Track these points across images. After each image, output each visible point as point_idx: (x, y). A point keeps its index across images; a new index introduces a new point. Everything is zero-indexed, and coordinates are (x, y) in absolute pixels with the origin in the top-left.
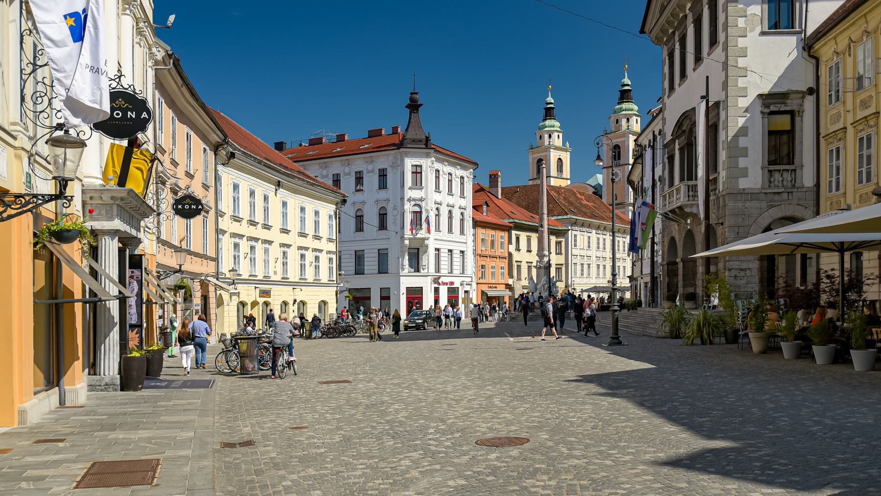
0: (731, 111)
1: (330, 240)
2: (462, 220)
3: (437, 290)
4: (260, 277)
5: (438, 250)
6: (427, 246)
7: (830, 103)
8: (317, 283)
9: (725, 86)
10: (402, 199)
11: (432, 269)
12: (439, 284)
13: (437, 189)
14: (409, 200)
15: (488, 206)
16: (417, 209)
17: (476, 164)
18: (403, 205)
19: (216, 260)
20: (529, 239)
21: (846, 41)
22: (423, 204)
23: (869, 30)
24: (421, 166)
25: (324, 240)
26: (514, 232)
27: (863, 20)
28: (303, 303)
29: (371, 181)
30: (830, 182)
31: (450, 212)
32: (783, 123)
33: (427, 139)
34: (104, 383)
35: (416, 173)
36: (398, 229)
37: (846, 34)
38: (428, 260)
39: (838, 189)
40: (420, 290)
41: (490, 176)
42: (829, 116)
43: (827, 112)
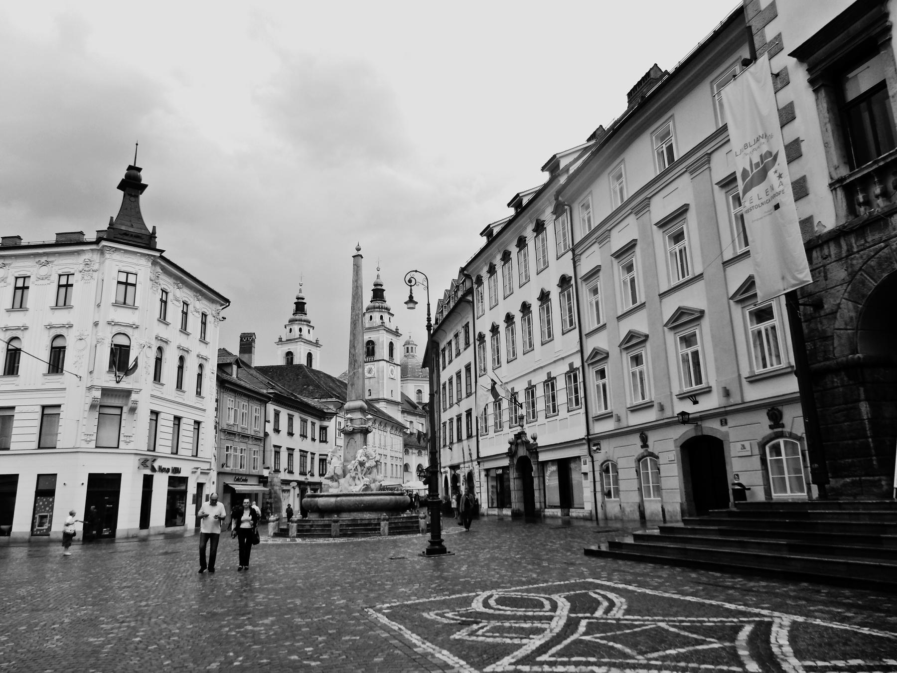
2: (200, 376)
3: (148, 482)
5: (156, 414)
11: (141, 443)
12: (153, 469)
13: (163, 318)
15: (239, 367)
17: (227, 301)
20: (291, 418)
26: (271, 408)
29: (42, 294)
31: (182, 359)
35: (127, 284)
36: (83, 373)
40: (115, 479)
41: (241, 340)
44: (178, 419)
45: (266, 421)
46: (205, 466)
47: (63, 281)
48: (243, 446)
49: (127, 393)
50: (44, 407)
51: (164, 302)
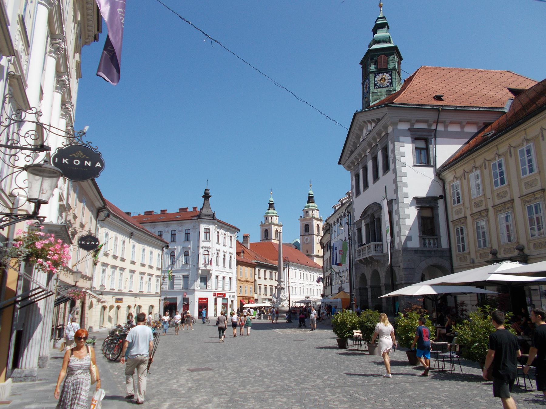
0: (400, 205)
1: (158, 269)
4: (116, 291)
6: (211, 274)
7: (454, 203)
8: (149, 295)
9: (396, 191)
10: (198, 247)
11: (214, 288)
14: (202, 248)
16: (206, 253)
17: (239, 230)
18: (198, 250)
19: (91, 279)
20: (265, 272)
21: (462, 172)
22: (210, 250)
23: (477, 166)
24: (209, 229)
25: (155, 269)
27: (473, 161)
28: (140, 307)
29: (180, 236)
30: (459, 246)
32: (427, 213)
33: (214, 215)
34: (23, 375)
37: (462, 168)
38: (212, 282)
39: (464, 250)
41: (244, 237)
42: (454, 210)
43: (452, 208)
44: (224, 277)
45: (255, 274)
46: (233, 294)
47: (187, 232)
48: (246, 285)
49: (209, 270)
50: (183, 276)
51: (218, 236)
